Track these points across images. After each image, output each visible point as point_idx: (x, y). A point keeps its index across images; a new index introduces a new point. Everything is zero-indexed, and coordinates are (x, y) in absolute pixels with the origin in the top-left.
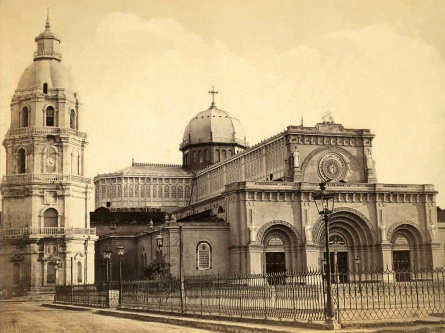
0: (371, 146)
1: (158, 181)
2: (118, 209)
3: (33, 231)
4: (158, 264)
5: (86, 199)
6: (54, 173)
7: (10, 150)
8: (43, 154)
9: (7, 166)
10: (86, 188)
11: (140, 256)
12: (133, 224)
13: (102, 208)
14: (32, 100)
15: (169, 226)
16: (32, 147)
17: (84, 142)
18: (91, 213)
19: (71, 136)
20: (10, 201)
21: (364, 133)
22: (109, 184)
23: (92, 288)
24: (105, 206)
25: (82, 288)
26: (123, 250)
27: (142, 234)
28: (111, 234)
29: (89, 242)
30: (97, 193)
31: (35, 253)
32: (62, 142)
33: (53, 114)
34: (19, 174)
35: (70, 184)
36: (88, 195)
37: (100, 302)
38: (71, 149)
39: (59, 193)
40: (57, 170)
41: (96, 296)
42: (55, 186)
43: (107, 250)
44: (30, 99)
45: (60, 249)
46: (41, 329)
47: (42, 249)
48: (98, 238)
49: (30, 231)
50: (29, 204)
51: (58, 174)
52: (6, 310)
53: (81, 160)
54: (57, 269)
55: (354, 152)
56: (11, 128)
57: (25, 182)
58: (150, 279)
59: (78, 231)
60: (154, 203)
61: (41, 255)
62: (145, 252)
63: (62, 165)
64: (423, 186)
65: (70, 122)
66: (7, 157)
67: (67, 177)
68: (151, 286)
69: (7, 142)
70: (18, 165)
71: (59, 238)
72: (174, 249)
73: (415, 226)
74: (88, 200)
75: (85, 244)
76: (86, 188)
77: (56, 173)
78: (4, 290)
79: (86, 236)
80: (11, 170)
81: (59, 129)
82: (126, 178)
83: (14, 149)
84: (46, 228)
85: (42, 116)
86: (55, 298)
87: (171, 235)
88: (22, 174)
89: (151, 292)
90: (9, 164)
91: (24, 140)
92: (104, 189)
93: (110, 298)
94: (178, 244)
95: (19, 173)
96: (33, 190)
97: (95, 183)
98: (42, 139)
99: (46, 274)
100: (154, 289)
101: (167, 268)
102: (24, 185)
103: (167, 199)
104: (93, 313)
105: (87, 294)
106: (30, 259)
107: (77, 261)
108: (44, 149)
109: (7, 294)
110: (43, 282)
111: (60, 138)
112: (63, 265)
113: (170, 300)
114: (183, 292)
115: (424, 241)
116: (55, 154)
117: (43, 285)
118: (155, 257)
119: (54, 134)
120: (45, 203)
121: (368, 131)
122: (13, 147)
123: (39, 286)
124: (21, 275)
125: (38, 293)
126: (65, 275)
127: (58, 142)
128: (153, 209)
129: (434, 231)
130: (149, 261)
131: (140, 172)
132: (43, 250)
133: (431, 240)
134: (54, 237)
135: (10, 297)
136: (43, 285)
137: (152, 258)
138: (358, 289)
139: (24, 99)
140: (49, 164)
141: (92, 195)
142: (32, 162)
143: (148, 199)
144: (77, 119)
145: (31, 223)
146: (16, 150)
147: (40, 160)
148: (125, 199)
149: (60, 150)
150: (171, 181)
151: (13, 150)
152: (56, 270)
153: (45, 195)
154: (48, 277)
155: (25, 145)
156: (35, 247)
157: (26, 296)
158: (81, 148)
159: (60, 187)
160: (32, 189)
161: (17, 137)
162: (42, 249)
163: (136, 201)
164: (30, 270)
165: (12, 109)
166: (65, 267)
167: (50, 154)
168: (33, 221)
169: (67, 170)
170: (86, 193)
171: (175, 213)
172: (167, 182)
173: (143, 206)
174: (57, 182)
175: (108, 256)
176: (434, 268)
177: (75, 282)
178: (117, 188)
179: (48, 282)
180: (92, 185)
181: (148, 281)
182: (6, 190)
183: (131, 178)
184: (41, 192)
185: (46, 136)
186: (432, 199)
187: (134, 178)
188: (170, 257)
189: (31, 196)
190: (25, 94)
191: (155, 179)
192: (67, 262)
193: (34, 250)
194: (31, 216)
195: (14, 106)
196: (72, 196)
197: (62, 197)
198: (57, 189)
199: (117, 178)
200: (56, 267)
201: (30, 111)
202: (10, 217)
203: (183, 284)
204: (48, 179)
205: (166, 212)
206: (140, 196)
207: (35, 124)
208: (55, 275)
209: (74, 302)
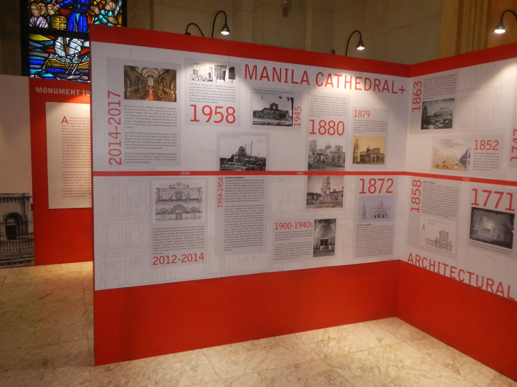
64: (24, 194)
73: (19, 213)
115: (24, 220)
133: (27, 220)
176: (29, 232)
186: (28, 200)
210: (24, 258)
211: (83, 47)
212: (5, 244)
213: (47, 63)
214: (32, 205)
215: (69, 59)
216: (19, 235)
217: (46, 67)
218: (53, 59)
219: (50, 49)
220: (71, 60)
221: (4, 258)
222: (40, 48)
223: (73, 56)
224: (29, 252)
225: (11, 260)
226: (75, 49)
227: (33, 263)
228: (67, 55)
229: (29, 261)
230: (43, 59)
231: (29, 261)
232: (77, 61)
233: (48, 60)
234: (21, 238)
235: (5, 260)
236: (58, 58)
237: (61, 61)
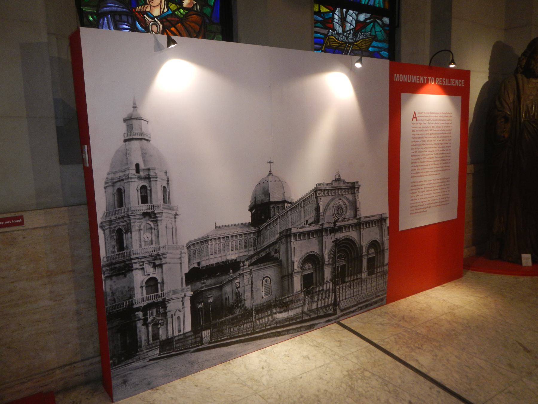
0: (359, 193)
1: (234, 237)
2: (207, 266)
3: (136, 301)
4: (237, 301)
5: (181, 263)
6: (151, 246)
7: (107, 231)
8: (140, 230)
9: (106, 247)
10: (181, 254)
11: (224, 298)
12: (218, 276)
13: (195, 268)
14: (125, 181)
15: (243, 271)
16: (129, 225)
17: (176, 215)
18: (186, 274)
19: (165, 211)
20: (111, 279)
21: (356, 184)
22: (199, 247)
23: (189, 334)
24: (196, 265)
25: (182, 336)
26: (212, 298)
27: (225, 282)
28: (202, 287)
29: (186, 298)
30: (189, 256)
31: (141, 319)
32: (156, 217)
33: (146, 192)
34: (119, 253)
35: (166, 253)
36: (182, 259)
37: (196, 343)
38: (165, 222)
39: (157, 262)
40: (154, 242)
41: (193, 339)
42: (153, 257)
43: (200, 301)
44: (123, 180)
45: (162, 310)
46: (149, 380)
47: (145, 315)
48: (192, 293)
49: (134, 302)
50: (130, 278)
51: (155, 246)
52: (117, 375)
53: (174, 231)
54: (160, 328)
55: (350, 197)
56: (107, 210)
57: (125, 259)
58: (232, 314)
59: (175, 292)
60: (232, 256)
61: (146, 320)
62: (228, 295)
63: (158, 237)
64: (382, 214)
65: (162, 198)
66: (105, 239)
67: (164, 247)
68: (233, 319)
69: (104, 224)
70: (117, 244)
71: (160, 301)
72: (248, 288)
74: (182, 264)
75: (182, 301)
76: (181, 254)
77: (154, 245)
78: (113, 359)
79: (183, 294)
80: (110, 250)
81: (153, 205)
82: (211, 240)
83: (112, 230)
84: (148, 296)
85: (136, 195)
86: (160, 351)
87: (245, 277)
88: (122, 252)
89: (233, 324)
90: (107, 245)
91: (121, 220)
92: (195, 252)
93: (203, 337)
94: (250, 283)
95: (118, 252)
96: (133, 265)
97: (188, 248)
98: (138, 217)
99: (150, 334)
100: (235, 322)
101: (243, 303)
102: (124, 262)
103: (241, 251)
104: (191, 353)
105: (186, 339)
106: (136, 325)
107: (177, 316)
108: (140, 226)
109: (116, 361)
110: (149, 341)
111: (155, 214)
112: (165, 322)
113: (245, 325)
114: (254, 317)
115: (382, 248)
116: (151, 228)
117: (149, 344)
118: (235, 297)
119: (149, 211)
120: (146, 274)
121: (357, 182)
122: (110, 228)
123: (145, 346)
124: (128, 341)
125: (145, 351)
126: (167, 330)
127: (154, 218)
128: (232, 260)
129: (386, 242)
130: (231, 301)
131: (221, 233)
132: (147, 315)
133: (384, 247)
134: (156, 302)
135: (119, 362)
136: (149, 344)
137: (233, 298)
138: (349, 286)
139: (117, 180)
140: (146, 239)
141: (185, 259)
142: (130, 240)
143: (228, 253)
144: (169, 195)
145: (134, 294)
146: (114, 231)
147: (138, 236)
148: (211, 257)
149: (156, 225)
150: (243, 236)
151: (110, 231)
152: (159, 328)
153: (144, 267)
154: (153, 337)
155: (122, 225)
156: (140, 314)
157: (135, 358)
158: (174, 220)
159: (158, 258)
160: (132, 264)
161: (113, 218)
162: (145, 315)
163: (219, 257)
164: (136, 335)
165: (105, 192)
166: (167, 324)
167: (147, 229)
168: (136, 292)
169: (163, 242)
170: (181, 258)
171: (247, 260)
172: (240, 238)
173: (224, 259)
174: (155, 253)
175: (201, 306)
176: (385, 264)
177: (176, 333)
178: (205, 249)
179: (153, 340)
180: (185, 250)
181: (231, 316)
182: (107, 270)
183: (215, 239)
184: (141, 265)
185: (141, 214)
186: (385, 222)
187: (217, 239)
188: (245, 294)
189: (132, 270)
190: (117, 175)
191: (232, 236)
192: (169, 319)
193: (139, 317)
194: (133, 288)
195: (108, 188)
196: (169, 263)
197: (160, 266)
198: (154, 260)
199: (204, 241)
200: (159, 326)
201: (124, 192)
202: (113, 293)
203: (254, 312)
204: (147, 252)
205: (240, 261)
206: (222, 252)
207: (130, 204)
208: (158, 333)
209: (176, 349)
210: (379, 296)
211: (357, 21)
212: (365, 281)
213: (327, 42)
214: (388, 227)
215: (346, 36)
216: (377, 268)
217: (326, 47)
218: (331, 37)
219: (330, 23)
220: (347, 38)
221: (364, 300)
222: (320, 22)
223: (349, 32)
224: (383, 289)
225: (368, 301)
226: (351, 24)
227: (385, 301)
228: (344, 31)
229: (382, 300)
230: (323, 36)
231: (382, 300)
232: (352, 39)
233: (327, 38)
234: (378, 271)
235: (364, 302)
236: (336, 36)
237: (338, 39)
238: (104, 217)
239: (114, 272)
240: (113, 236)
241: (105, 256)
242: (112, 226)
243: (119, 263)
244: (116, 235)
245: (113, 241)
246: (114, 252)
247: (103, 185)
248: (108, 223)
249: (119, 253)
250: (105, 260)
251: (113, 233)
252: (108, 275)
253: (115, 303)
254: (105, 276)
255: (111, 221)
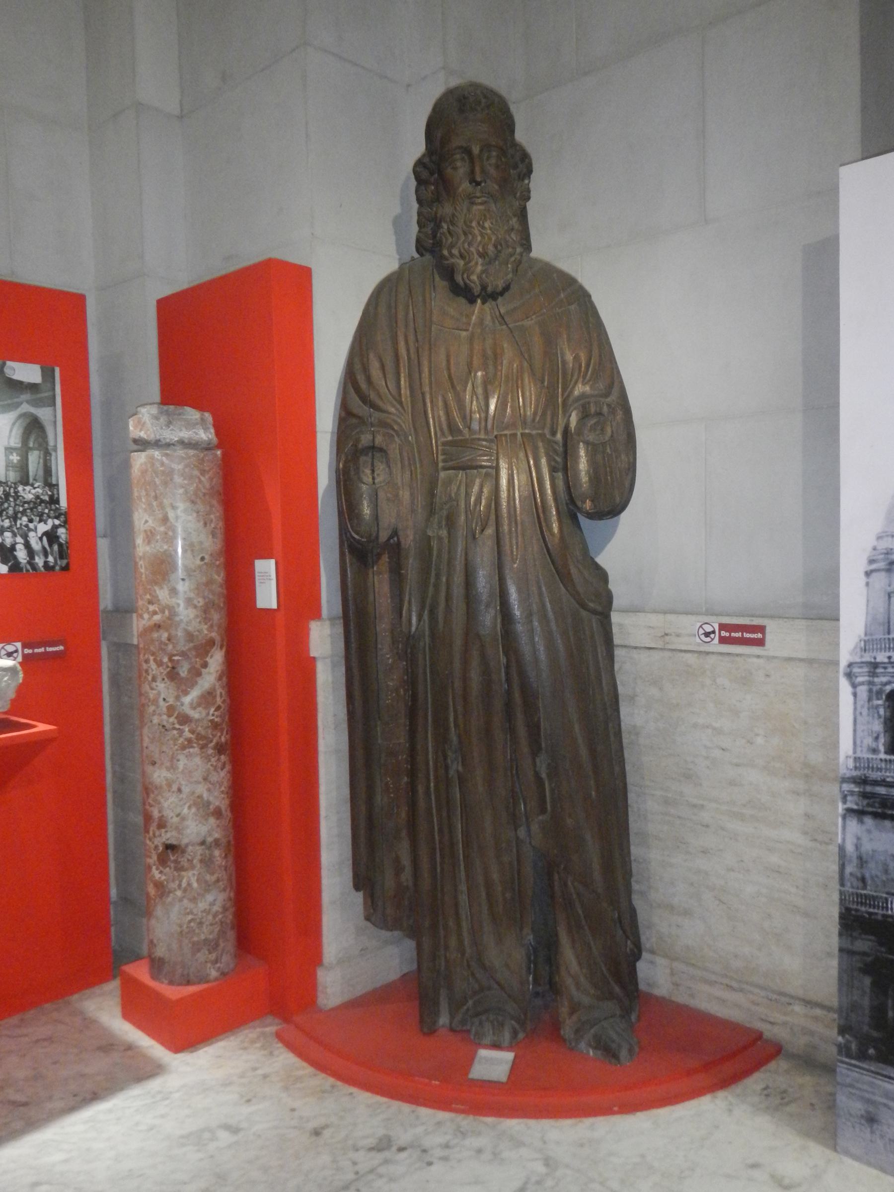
7: (863, 690)
9: (855, 731)
20: (861, 822)
34: (888, 757)
56: (866, 634)
66: (855, 709)
69: (856, 670)
83: (875, 689)
90: (860, 727)
95: (886, 753)
122: (871, 683)
146: (879, 693)
151: (870, 691)
161: (882, 657)
165: (867, 584)
182: (852, 793)
195: (874, 575)
238: (858, 650)
239: (868, 805)
240: (877, 707)
241: (850, 753)
242: (876, 680)
243: (885, 786)
244: (884, 705)
245: (876, 722)
246: (875, 751)
247: (863, 566)
248: (866, 669)
249: (888, 757)
250: (851, 764)
251: (878, 699)
252: (855, 807)
253: (865, 888)
254: (845, 806)
255: (875, 665)
